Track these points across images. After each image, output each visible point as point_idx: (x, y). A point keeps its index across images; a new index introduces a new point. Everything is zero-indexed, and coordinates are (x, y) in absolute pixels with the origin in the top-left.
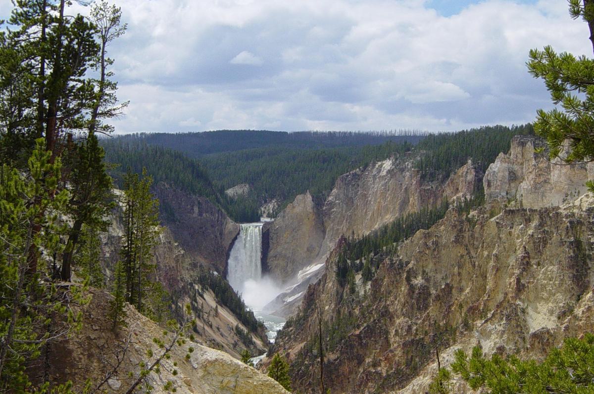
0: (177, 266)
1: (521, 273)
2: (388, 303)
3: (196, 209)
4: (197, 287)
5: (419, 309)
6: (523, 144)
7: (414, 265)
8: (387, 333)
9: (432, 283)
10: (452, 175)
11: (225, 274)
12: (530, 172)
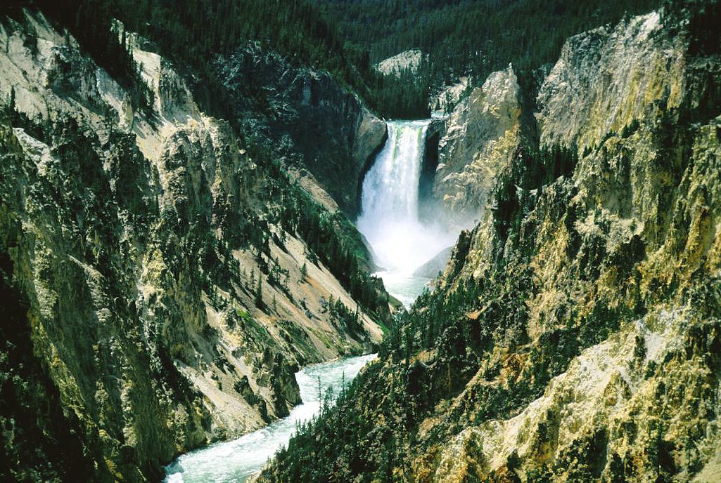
3: (307, 93)
4: (273, 229)
5: (583, 278)
7: (584, 198)
8: (525, 318)
9: (612, 233)
11: (352, 207)
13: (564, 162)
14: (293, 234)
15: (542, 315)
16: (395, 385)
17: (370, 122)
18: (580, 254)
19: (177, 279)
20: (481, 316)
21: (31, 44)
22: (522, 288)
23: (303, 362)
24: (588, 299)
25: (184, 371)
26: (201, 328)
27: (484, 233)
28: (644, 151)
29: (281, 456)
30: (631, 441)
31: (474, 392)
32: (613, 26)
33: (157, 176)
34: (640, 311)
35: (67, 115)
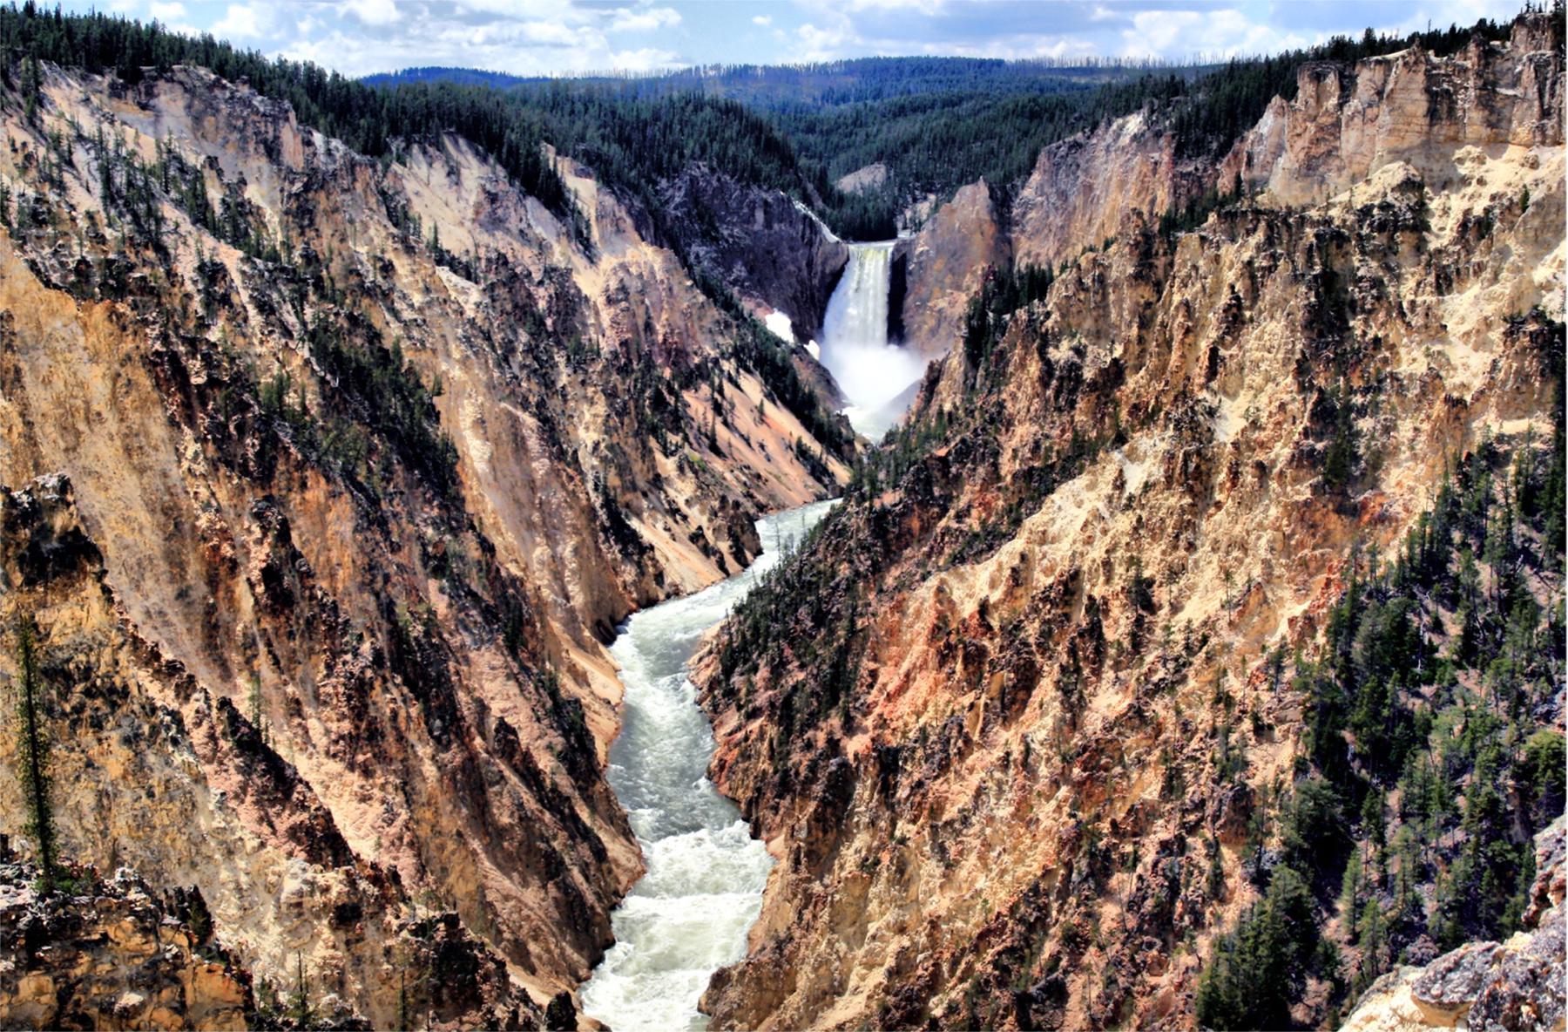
1: (1222, 339)
2: (1004, 396)
3: (760, 215)
5: (1059, 410)
6: (1318, 78)
9: (1088, 360)
10: (1237, 144)
12: (1299, 135)
13: (1038, 283)
14: (748, 371)
16: (858, 530)
18: (1054, 383)
20: (949, 453)
21: (453, 172)
22: (992, 421)
23: (762, 508)
24: (1063, 431)
25: (634, 523)
26: (651, 476)
28: (1121, 265)
29: (739, 610)
30: (1108, 581)
31: (943, 535)
32: (1092, 131)
33: (597, 313)
34: (1121, 439)
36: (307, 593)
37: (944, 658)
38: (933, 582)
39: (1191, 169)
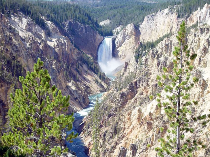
0: (71, 53)
3: (84, 30)
8: (148, 81)
10: (191, 15)
14: (84, 63)
15: (152, 80)
17: (99, 37)
19: (60, 74)
20: (137, 80)
26: (66, 86)
27: (132, 62)
35: (30, 36)
36: (4, 110)
37: (142, 124)
38: (137, 108)
39: (181, 20)
